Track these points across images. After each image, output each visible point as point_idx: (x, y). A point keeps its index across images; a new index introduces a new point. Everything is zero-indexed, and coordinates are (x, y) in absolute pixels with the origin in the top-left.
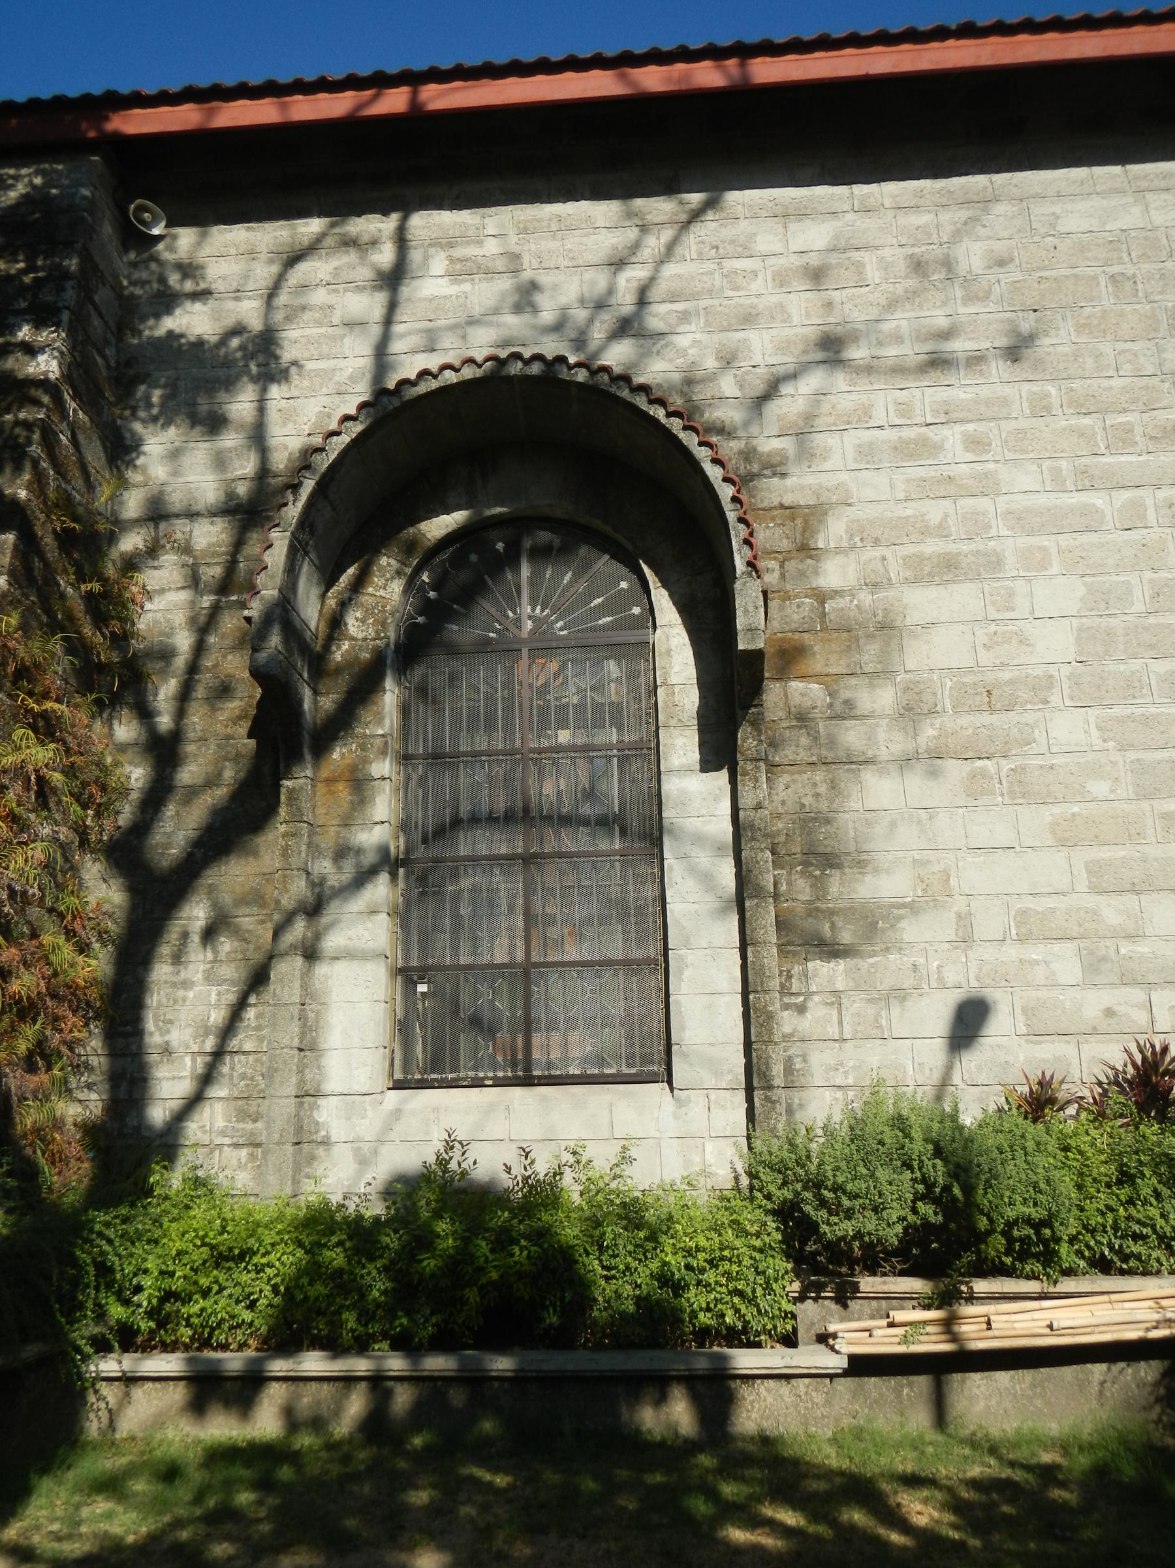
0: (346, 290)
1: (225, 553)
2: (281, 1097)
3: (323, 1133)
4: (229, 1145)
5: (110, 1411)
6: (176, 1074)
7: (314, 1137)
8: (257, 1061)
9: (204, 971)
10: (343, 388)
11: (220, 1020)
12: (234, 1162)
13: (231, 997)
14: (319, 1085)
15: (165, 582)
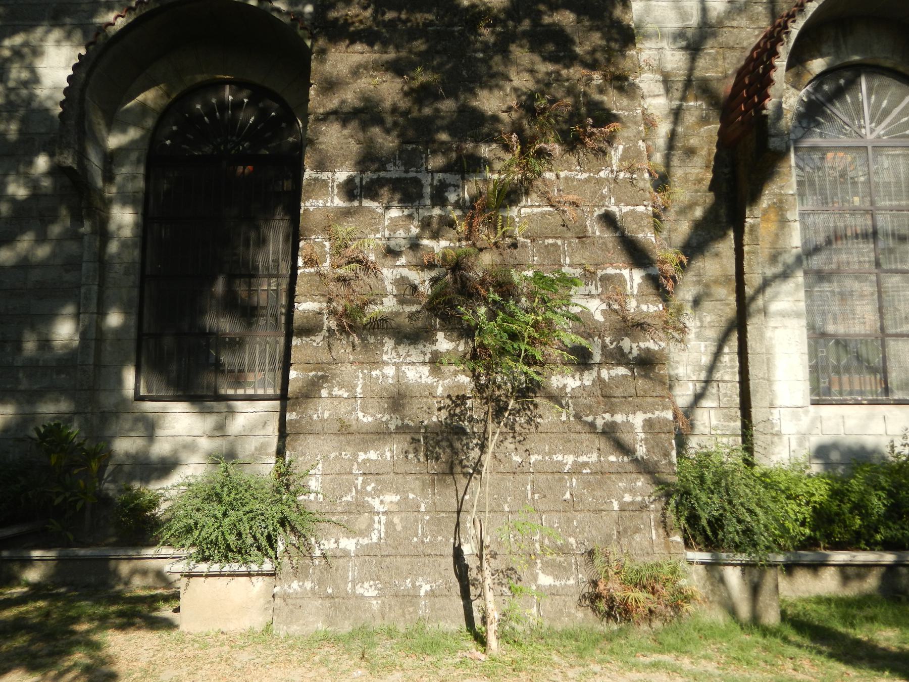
1: (684, 75)
6: (684, 393)
8: (733, 386)
9: (695, 333)
11: (708, 362)
13: (713, 348)
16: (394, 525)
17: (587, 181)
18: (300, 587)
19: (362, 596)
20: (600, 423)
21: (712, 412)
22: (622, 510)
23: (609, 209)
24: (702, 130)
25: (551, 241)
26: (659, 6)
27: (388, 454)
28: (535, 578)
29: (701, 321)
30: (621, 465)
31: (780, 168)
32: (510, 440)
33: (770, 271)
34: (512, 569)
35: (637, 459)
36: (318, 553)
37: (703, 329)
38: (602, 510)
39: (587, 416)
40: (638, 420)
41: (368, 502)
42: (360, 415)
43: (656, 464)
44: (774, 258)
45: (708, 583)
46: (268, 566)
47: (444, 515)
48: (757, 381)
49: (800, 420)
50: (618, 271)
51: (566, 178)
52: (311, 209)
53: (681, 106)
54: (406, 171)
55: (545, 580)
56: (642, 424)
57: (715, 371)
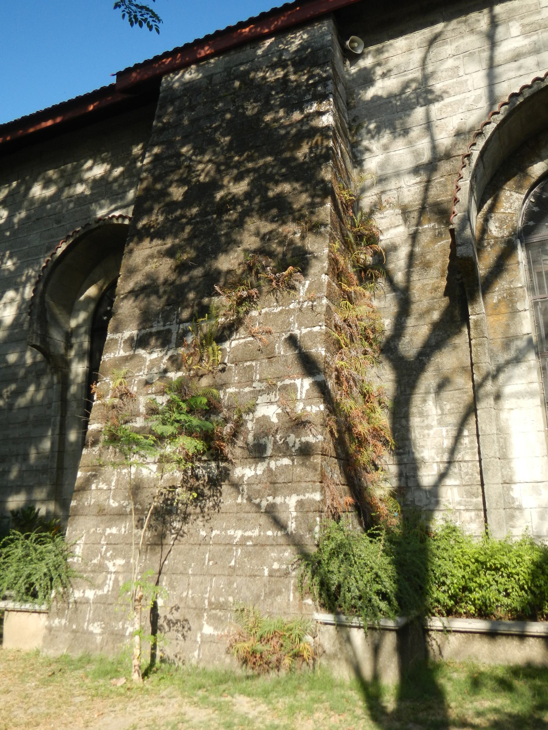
0: (464, 57)
1: (419, 205)
2: (494, 484)
3: (517, 503)
4: (464, 510)
5: (439, 646)
6: (430, 473)
7: (512, 505)
8: (473, 465)
9: (437, 420)
10: (471, 107)
11: (450, 445)
12: (468, 519)
13: (453, 432)
14: (511, 477)
15: (388, 224)
17: (281, 312)
19: (91, 633)
20: (264, 504)
21: (455, 490)
22: (270, 576)
23: (293, 333)
24: (436, 246)
26: (396, 155)
27: (123, 530)
28: (201, 628)
29: (442, 409)
30: (274, 538)
31: (508, 265)
32: (201, 519)
33: (502, 358)
34: (186, 620)
35: (287, 534)
37: (444, 416)
38: (255, 576)
39: (256, 499)
40: (292, 501)
42: (111, 501)
43: (301, 538)
44: (507, 345)
45: (337, 642)
46: (44, 607)
48: (488, 460)
49: (540, 495)
50: (293, 381)
51: (266, 313)
53: (417, 230)
55: (208, 630)
56: (295, 504)
57: (456, 452)
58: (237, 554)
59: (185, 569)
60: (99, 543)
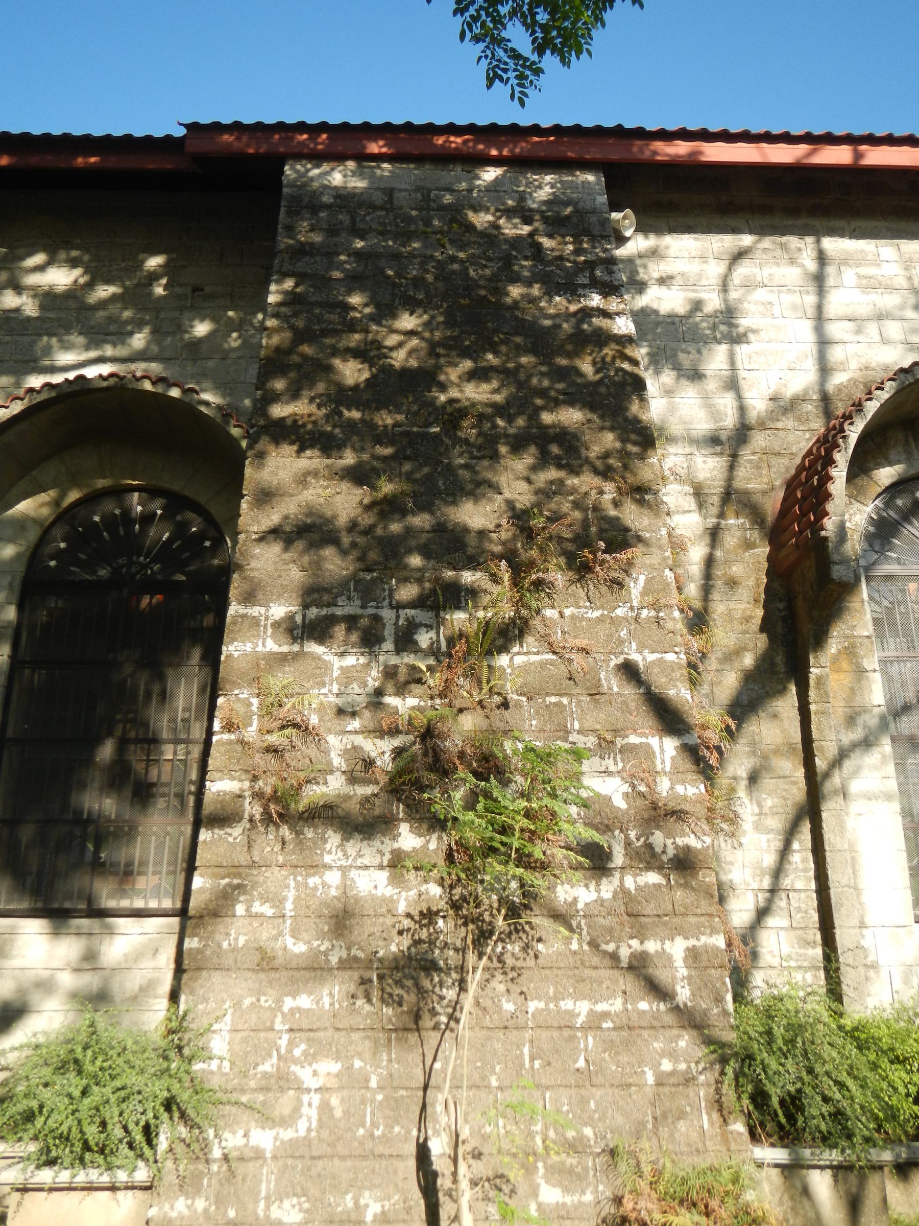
1: (720, 487)
10: (793, 366)
11: (772, 863)
13: (778, 844)
16: (331, 1109)
17: (600, 620)
18: (189, 1207)
20: (624, 953)
21: (782, 934)
22: (659, 1084)
23: (630, 657)
25: (553, 699)
27: (326, 1001)
28: (535, 1193)
29: (760, 806)
30: (656, 1016)
32: (499, 977)
34: (502, 1176)
35: (677, 1008)
36: (217, 1153)
39: (607, 943)
40: (677, 948)
41: (295, 1074)
42: (289, 941)
43: (705, 1015)
44: (851, 720)
45: (786, 1197)
46: (142, 1174)
47: (403, 1093)
48: (840, 890)
50: (643, 740)
51: (572, 617)
52: (236, 654)
53: (718, 524)
54: (363, 607)
55: (550, 1194)
56: (683, 955)
57: (782, 875)
58: (586, 1046)
59: (484, 1077)
60: (272, 1029)
